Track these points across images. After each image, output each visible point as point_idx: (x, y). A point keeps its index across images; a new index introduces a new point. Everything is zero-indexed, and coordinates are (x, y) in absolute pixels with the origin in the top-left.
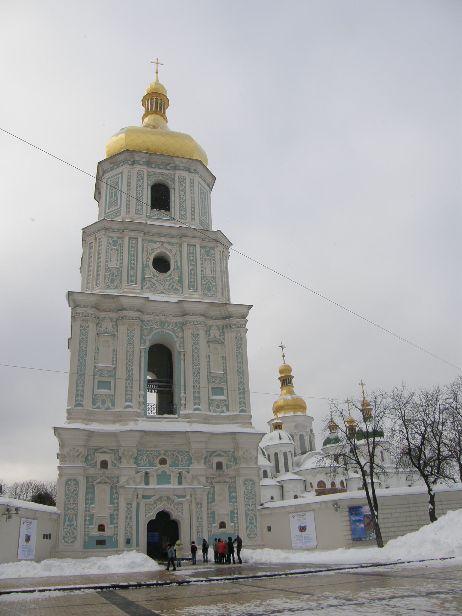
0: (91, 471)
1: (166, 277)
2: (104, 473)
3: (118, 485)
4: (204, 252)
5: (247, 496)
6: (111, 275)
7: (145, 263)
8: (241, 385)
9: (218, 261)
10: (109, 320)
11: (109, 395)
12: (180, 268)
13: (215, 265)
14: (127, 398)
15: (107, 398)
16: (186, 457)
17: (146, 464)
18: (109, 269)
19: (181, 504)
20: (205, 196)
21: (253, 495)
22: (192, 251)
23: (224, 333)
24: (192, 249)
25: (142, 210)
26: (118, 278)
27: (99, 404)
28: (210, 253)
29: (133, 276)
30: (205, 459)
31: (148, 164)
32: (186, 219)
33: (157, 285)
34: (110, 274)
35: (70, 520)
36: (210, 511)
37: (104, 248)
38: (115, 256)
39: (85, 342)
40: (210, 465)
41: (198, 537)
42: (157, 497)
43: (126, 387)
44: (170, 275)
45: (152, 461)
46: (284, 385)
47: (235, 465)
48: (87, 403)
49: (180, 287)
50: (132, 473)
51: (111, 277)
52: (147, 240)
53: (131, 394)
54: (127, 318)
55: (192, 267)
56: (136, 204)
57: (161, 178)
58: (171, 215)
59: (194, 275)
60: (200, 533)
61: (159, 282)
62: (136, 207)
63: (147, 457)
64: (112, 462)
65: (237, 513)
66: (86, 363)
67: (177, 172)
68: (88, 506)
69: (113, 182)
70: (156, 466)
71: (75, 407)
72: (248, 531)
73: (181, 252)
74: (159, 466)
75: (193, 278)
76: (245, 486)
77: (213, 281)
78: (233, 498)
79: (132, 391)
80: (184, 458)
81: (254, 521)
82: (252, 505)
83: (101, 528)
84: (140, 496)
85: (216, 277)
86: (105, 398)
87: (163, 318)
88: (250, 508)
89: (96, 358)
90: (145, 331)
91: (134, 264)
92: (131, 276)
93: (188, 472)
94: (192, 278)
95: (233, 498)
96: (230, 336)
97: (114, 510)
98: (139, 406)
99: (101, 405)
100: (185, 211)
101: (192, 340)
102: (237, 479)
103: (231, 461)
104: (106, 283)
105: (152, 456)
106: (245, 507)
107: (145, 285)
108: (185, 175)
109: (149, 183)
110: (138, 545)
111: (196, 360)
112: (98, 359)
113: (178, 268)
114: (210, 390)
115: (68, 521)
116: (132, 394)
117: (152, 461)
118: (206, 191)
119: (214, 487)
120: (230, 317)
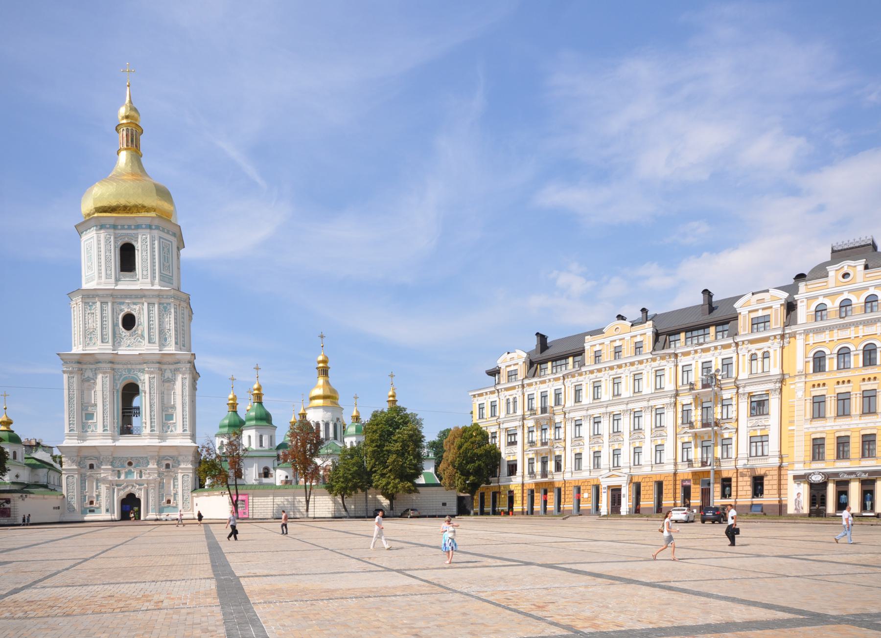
4: (162, 308)
7: (115, 322)
30: (158, 462)
51: (89, 336)
57: (126, 240)
58: (136, 275)
73: (143, 309)
87: (129, 366)
90: (117, 377)
100: (147, 270)
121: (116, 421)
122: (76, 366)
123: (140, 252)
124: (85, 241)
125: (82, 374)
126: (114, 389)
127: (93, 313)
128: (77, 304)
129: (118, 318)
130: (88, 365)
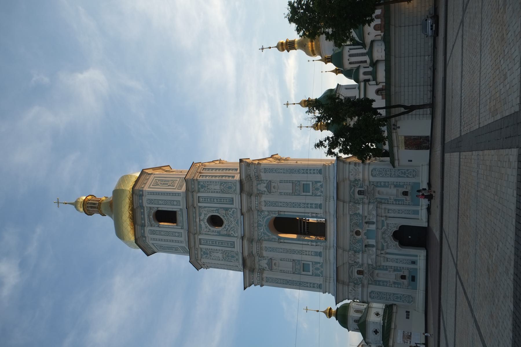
0: (365, 282)
1: (225, 219)
3: (374, 265)
4: (203, 190)
5: (384, 176)
6: (229, 257)
7: (216, 234)
8: (300, 171)
10: (261, 261)
11: (312, 265)
12: (217, 208)
13: (211, 182)
14: (314, 255)
15: (314, 267)
16: (355, 217)
17: (360, 245)
18: (225, 258)
19: (388, 224)
21: (383, 170)
22: (204, 200)
23: (262, 180)
24: (201, 200)
25: (178, 232)
26: (230, 253)
27: (318, 272)
28: (202, 185)
29: (227, 243)
31: (143, 226)
32: (180, 201)
33: (232, 226)
34: (228, 258)
35: (397, 298)
36: (394, 202)
38: (215, 254)
39: (277, 280)
40: (360, 200)
41: (412, 214)
42: (382, 241)
43: (306, 255)
44: (224, 216)
45: (357, 241)
46: (294, 48)
47: (360, 180)
48: (318, 280)
49: (231, 210)
50: (365, 255)
53: (310, 252)
54: (258, 251)
55: (215, 200)
56: (174, 236)
57: (151, 217)
58: (178, 211)
59: (221, 199)
60: (410, 212)
61: (230, 225)
62: (177, 236)
63: (355, 244)
64: (358, 267)
65: (397, 182)
66: (291, 280)
67: (144, 205)
68: (388, 285)
69: (161, 248)
71: (322, 289)
72: (410, 176)
73: (205, 207)
75: (223, 200)
76: (377, 176)
77: (223, 185)
78: (386, 185)
79: (309, 251)
80: (355, 218)
81: (403, 171)
82: (391, 172)
83: (403, 277)
84: (382, 252)
85: (220, 182)
86: (315, 268)
87: (256, 225)
88: (393, 173)
89: (287, 272)
90: (266, 238)
91: (219, 242)
92: (228, 245)
93: (366, 217)
94: (224, 201)
95: (386, 185)
96: (264, 176)
97: (392, 268)
98: (319, 246)
99: (319, 271)
100: (174, 201)
101: (270, 206)
102: (371, 180)
103: (358, 183)
104: (235, 261)
105: (354, 240)
106: (392, 177)
107: (233, 235)
108: (146, 200)
109: (157, 226)
110: (416, 256)
111: (284, 204)
112: (288, 271)
113: (218, 210)
114: (305, 194)
115: (398, 299)
116: (311, 251)
117: (357, 241)
119: (376, 198)
120: (250, 175)
121: (310, 243)
122: (256, 275)
124: (158, 250)
125: (264, 270)
126: (278, 242)
127: (210, 252)
128: (204, 264)
129: (213, 231)
130: (256, 262)
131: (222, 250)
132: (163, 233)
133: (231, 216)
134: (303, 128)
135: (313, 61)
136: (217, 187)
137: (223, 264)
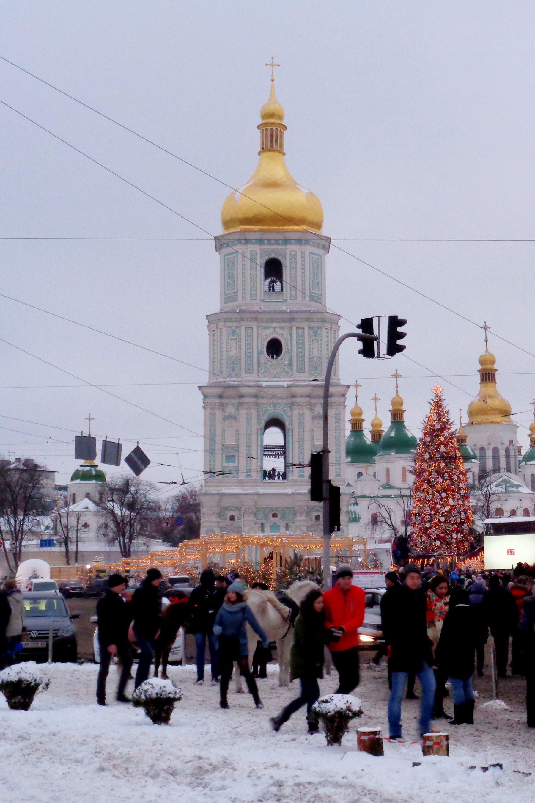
2: (232, 524)
4: (312, 332)
7: (259, 350)
9: (325, 339)
18: (230, 359)
20: (318, 264)
24: (300, 332)
31: (260, 242)
37: (224, 338)
46: (483, 380)
51: (231, 366)
52: (262, 327)
55: (300, 350)
57: (273, 256)
58: (283, 296)
59: (302, 358)
70: (270, 519)
73: (291, 335)
74: (272, 519)
90: (261, 413)
105: (266, 511)
113: (288, 352)
118: (318, 257)
122: (217, 400)
123: (288, 268)
124: (225, 255)
131: (240, 355)
132: (253, 272)
133: (282, 369)
134: (355, 389)
135: (461, 417)
136: (315, 353)
137: (221, 356)
